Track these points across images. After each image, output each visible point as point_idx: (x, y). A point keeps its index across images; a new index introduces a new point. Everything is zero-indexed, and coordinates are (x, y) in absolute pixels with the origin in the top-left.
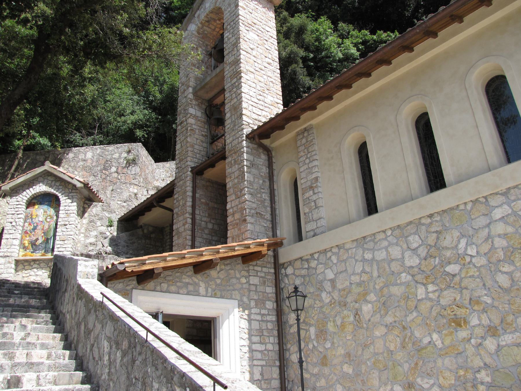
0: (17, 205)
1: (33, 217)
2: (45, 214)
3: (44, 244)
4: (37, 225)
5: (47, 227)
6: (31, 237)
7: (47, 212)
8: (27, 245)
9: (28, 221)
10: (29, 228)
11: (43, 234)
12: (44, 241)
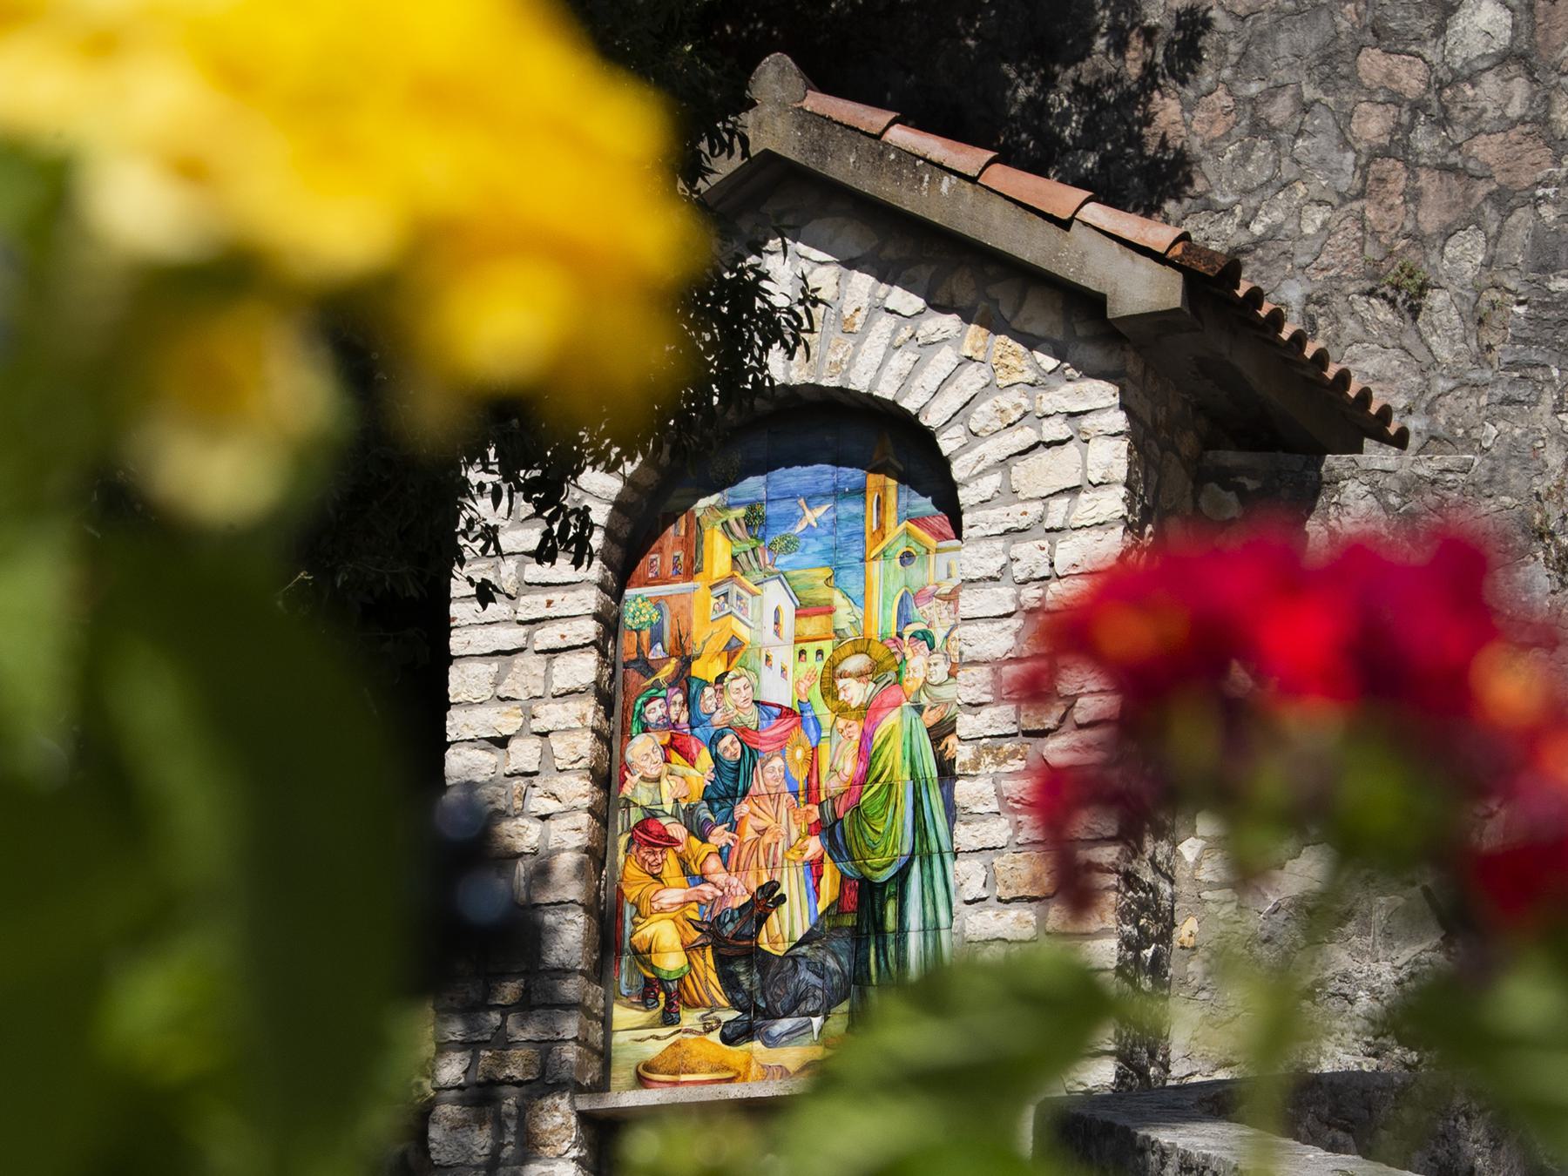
1: (697, 669)
2: (813, 626)
3: (841, 944)
4: (751, 754)
5: (849, 766)
6: (703, 879)
7: (829, 610)
8: (671, 961)
9: (655, 712)
10: (668, 789)
11: (814, 846)
12: (836, 908)
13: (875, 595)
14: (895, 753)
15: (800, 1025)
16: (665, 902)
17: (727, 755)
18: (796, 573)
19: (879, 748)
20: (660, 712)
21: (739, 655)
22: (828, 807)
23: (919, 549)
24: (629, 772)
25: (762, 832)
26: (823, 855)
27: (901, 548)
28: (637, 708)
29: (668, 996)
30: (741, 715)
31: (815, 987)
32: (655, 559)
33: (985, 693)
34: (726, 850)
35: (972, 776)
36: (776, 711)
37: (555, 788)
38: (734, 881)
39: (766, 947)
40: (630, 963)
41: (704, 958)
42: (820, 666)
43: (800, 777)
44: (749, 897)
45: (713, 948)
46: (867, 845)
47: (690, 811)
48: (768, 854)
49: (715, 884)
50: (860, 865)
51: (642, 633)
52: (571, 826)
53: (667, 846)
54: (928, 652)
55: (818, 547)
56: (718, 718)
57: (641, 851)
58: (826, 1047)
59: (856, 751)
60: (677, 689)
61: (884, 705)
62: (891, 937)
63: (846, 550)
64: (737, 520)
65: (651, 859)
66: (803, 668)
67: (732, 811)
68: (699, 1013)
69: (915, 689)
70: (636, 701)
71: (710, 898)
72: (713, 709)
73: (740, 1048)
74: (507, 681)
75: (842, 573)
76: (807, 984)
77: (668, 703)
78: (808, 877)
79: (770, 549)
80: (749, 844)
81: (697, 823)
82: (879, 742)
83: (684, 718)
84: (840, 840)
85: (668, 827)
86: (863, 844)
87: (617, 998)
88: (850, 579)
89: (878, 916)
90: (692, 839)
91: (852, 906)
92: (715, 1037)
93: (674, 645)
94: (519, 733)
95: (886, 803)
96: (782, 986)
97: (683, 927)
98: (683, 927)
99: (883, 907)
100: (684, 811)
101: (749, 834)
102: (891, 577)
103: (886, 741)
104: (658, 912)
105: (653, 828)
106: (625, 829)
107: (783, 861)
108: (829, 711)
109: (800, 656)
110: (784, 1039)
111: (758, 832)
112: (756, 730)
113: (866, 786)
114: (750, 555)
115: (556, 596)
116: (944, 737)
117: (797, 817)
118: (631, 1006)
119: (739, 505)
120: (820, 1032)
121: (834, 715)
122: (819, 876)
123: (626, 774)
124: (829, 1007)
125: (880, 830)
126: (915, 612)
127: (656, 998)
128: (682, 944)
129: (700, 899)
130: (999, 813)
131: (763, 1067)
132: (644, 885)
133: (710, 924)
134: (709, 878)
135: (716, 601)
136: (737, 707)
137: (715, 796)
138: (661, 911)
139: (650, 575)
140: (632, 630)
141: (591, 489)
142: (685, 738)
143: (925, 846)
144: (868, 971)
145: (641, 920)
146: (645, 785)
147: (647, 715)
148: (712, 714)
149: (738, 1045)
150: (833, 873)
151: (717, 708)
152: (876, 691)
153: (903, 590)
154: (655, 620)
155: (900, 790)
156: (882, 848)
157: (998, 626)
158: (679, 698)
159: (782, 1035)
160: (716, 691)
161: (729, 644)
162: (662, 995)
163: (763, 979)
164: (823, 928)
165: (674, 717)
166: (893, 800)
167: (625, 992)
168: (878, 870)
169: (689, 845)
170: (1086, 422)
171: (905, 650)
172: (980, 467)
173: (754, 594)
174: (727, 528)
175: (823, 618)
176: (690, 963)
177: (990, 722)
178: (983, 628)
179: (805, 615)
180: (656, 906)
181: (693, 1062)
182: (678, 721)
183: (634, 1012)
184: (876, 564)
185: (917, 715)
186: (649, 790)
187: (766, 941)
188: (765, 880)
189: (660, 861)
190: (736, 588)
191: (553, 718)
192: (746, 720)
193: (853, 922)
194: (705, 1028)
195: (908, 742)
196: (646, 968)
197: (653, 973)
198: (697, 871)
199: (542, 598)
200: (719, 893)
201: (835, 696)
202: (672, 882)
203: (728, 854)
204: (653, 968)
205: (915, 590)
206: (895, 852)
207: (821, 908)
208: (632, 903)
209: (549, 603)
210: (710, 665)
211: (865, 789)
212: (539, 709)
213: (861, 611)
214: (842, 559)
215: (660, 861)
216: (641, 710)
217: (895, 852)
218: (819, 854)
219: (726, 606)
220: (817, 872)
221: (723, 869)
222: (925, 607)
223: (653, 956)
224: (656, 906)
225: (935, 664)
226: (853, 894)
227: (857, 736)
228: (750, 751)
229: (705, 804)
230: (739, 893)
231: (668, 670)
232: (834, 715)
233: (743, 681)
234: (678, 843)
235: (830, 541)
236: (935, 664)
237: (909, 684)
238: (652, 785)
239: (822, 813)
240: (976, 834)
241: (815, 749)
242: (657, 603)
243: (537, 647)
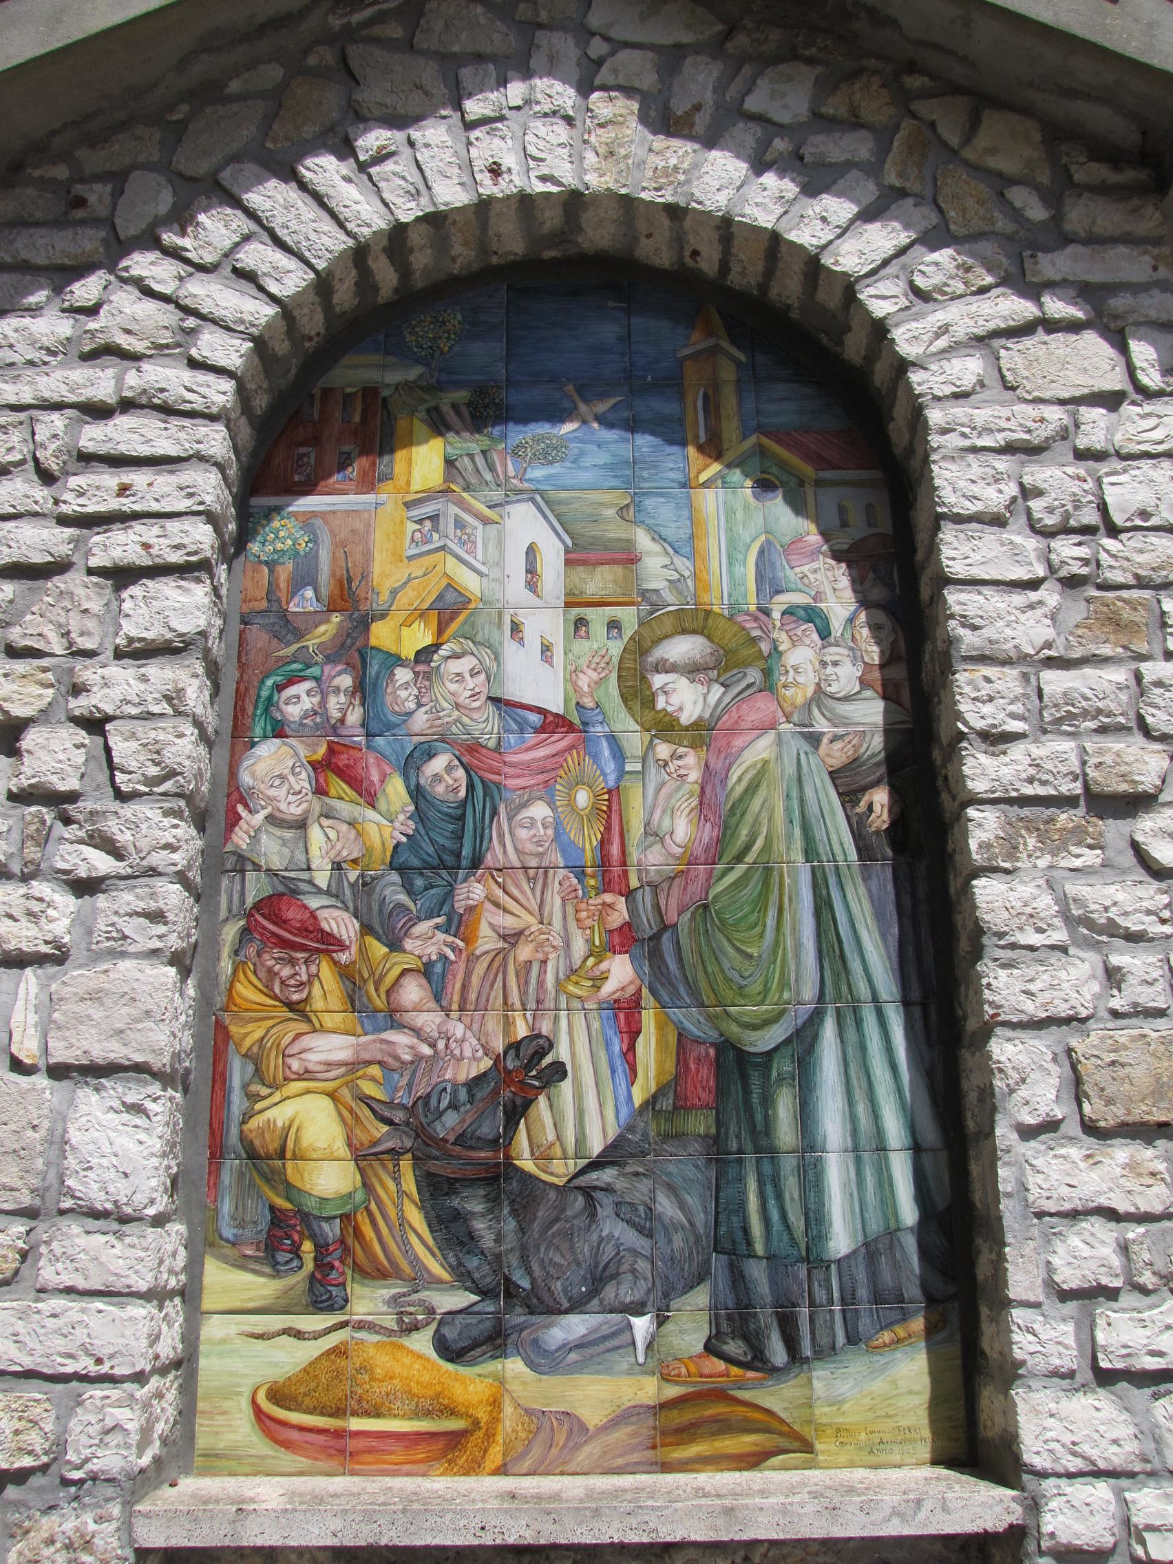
0: (97, 411)
1: (381, 634)
2: (599, 582)
6: (393, 1018)
7: (630, 559)
13: (713, 542)
14: (772, 810)
15: (606, 1330)
16: (313, 1058)
17: (440, 789)
18: (564, 494)
19: (741, 799)
20: (307, 703)
21: (460, 619)
22: (645, 899)
23: (785, 477)
24: (246, 806)
25: (513, 938)
26: (640, 989)
28: (265, 693)
29: (321, 1249)
30: (466, 720)
31: (635, 1253)
32: (305, 455)
33: (1013, 716)
34: (438, 968)
35: (1007, 872)
36: (535, 718)
37: (112, 827)
38: (459, 1030)
39: (527, 1165)
40: (241, 1175)
41: (397, 1180)
42: (615, 649)
43: (588, 841)
44: (487, 1063)
45: (415, 1158)
46: (729, 980)
47: (366, 885)
48: (527, 982)
49: (417, 1032)
50: (717, 1016)
51: (279, 568)
52: (141, 906)
53: (318, 951)
54: (819, 642)
55: (603, 458)
56: (420, 720)
57: (266, 956)
58: (666, 1378)
59: (695, 802)
60: (340, 667)
61: (743, 725)
62: (788, 1163)
63: (654, 467)
64: (455, 406)
65: (286, 972)
66: (582, 647)
67: (450, 894)
68: (386, 1292)
69: (799, 700)
70: (262, 682)
71: (407, 1058)
72: (412, 705)
73: (477, 1369)
74: (29, 617)
75: (649, 502)
76: (618, 1246)
77: (323, 689)
78: (611, 1032)
79: (515, 454)
80: (488, 959)
81: (381, 910)
82: (739, 790)
83: (354, 716)
84: (672, 965)
85: (322, 914)
86: (720, 977)
87: (212, 1245)
88: (663, 510)
89: (759, 1117)
90: (371, 941)
91: (704, 1095)
92: (422, 1342)
93: (337, 592)
94: (43, 716)
95: (761, 902)
96: (565, 1246)
97: (351, 1111)
98: (351, 1111)
99: (768, 1101)
100: (352, 885)
101: (487, 941)
102: (740, 515)
103: (752, 788)
104: (300, 1078)
105: (291, 914)
106: (235, 910)
107: (556, 1000)
108: (638, 728)
109: (577, 628)
110: (573, 1356)
111: (504, 938)
112: (497, 749)
113: (720, 867)
114: (480, 460)
115: (138, 478)
116: (864, 789)
117: (584, 915)
118: (241, 1263)
119: (458, 385)
120: (649, 1347)
121: (647, 736)
122: (633, 1033)
123: (240, 808)
124: (666, 1295)
125: (754, 951)
126: (791, 575)
127: (296, 1251)
128: (350, 1145)
129: (390, 1060)
130: (1064, 949)
131: (529, 1412)
132: (271, 1022)
133: (411, 1110)
134: (408, 1017)
135: (418, 527)
136: (457, 706)
137: (416, 862)
138: (306, 1075)
139: (296, 478)
140: (260, 562)
141: (218, 313)
142: (359, 755)
143: (844, 988)
144: (746, 1231)
145: (264, 1091)
146: (278, 832)
147: (283, 707)
148: (410, 714)
149: (473, 1363)
150: (660, 1027)
151: (419, 705)
152: (727, 699)
153: (763, 538)
154: (302, 548)
155: (787, 881)
156: (758, 987)
157: (1018, 599)
158: (346, 681)
159: (567, 1347)
160: (416, 674)
161: (440, 597)
162: (307, 1246)
163: (522, 1230)
164: (645, 1134)
165: (335, 714)
166: (774, 897)
167: (228, 1233)
168: (755, 1027)
169: (363, 950)
170: (1118, 303)
171: (775, 635)
172: (942, 343)
173: (486, 521)
175: (619, 570)
176: (365, 1185)
177: (1032, 771)
178: (997, 601)
179: (584, 563)
180: (295, 1065)
181: (380, 1389)
182: (342, 721)
183: (248, 1277)
184: (710, 494)
185: (805, 747)
186: (284, 842)
187: (527, 1153)
188: (522, 1031)
189: (304, 978)
190: (454, 510)
191: (116, 693)
192: (476, 729)
193: (709, 1127)
194: (400, 1321)
195: (795, 793)
196: (273, 1188)
197: (288, 1199)
198: (379, 1003)
199: (109, 480)
200: (426, 1050)
202: (329, 1020)
203: (444, 976)
204: (289, 1190)
205: (787, 540)
206: (786, 996)
207: (639, 1095)
208: (245, 1056)
209: (123, 490)
210: (405, 630)
211: (716, 873)
212: (88, 673)
213: (688, 563)
214: (645, 480)
215: (304, 978)
216: (270, 697)
217: (786, 996)
218: (631, 990)
219: (436, 536)
220: (628, 1024)
221: (433, 1005)
222: (805, 569)
223: (289, 1164)
224: (295, 1065)
225: (835, 664)
226: (704, 1072)
227: (694, 776)
228: (483, 782)
229: (395, 877)
230: (468, 1053)
231: (326, 631)
232: (647, 736)
233: (465, 664)
234: (343, 947)
236: (835, 664)
237: (789, 693)
238: (289, 834)
239: (632, 911)
240: (1032, 987)
241: (614, 793)
243: (94, 562)
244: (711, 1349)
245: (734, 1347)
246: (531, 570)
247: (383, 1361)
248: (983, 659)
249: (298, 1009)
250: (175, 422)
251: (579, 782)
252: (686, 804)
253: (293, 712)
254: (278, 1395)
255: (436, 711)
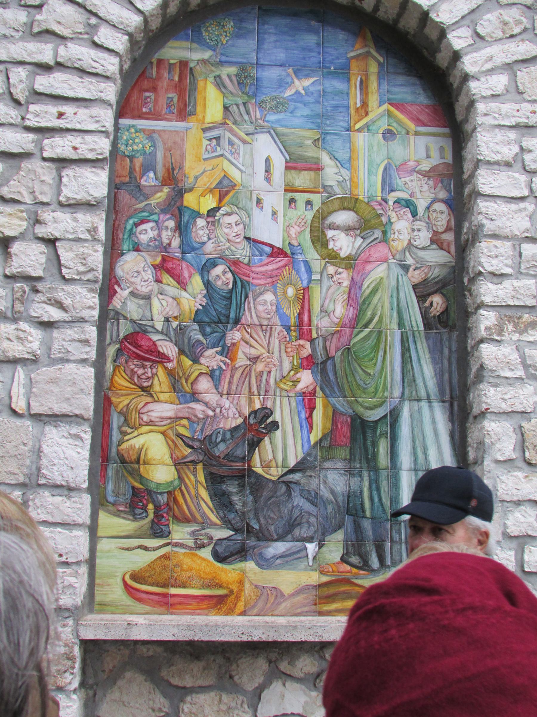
0: (45, 68)
1: (189, 200)
6: (194, 397)
7: (318, 169)
13: (361, 162)
14: (383, 303)
15: (294, 549)
16: (154, 415)
17: (219, 283)
18: (286, 130)
19: (368, 297)
20: (152, 234)
21: (231, 194)
22: (319, 344)
23: (399, 129)
24: (119, 286)
25: (254, 360)
26: (315, 388)
27: (383, 125)
28: (129, 227)
29: (157, 508)
30: (233, 248)
31: (310, 514)
32: (148, 97)
33: (507, 265)
34: (217, 373)
35: (497, 341)
36: (268, 249)
37: (61, 296)
38: (227, 404)
39: (259, 470)
40: (117, 471)
41: (195, 476)
42: (310, 215)
43: (293, 313)
44: (240, 420)
45: (204, 465)
46: (358, 385)
47: (181, 330)
48: (261, 382)
49: (206, 404)
50: (352, 402)
51: (136, 160)
52: (77, 337)
53: (157, 362)
54: (412, 219)
55: (306, 112)
56: (210, 247)
57: (130, 363)
58: (322, 573)
59: (346, 297)
60: (168, 216)
61: (372, 259)
62: (383, 474)
63: (334, 119)
64: (229, 76)
65: (141, 371)
66: (292, 213)
67: (223, 336)
68: (189, 529)
69: (400, 248)
70: (127, 221)
71: (201, 416)
72: (205, 239)
73: (232, 566)
74: (12, 182)
75: (329, 138)
76: (301, 510)
78: (301, 408)
79: (261, 106)
80: (242, 369)
81: (189, 343)
82: (368, 292)
83: (176, 243)
84: (332, 377)
85: (159, 343)
86: (354, 383)
87: (102, 505)
89: (370, 451)
90: (183, 358)
91: (344, 440)
92: (206, 553)
93: (166, 175)
94: (21, 237)
95: (376, 348)
96: (276, 510)
97: (173, 441)
98: (173, 441)
99: (375, 444)
100: (175, 330)
101: (241, 361)
102: (375, 148)
103: (375, 291)
104: (147, 424)
105: (143, 342)
106: (114, 339)
107: (275, 390)
108: (319, 257)
109: (290, 204)
110: (278, 561)
111: (250, 359)
112: (248, 265)
113: (356, 330)
114: (242, 108)
115: (69, 109)
116: (429, 295)
117: (289, 350)
118: (118, 514)
120: (315, 558)
121: (324, 262)
122: (311, 408)
123: (116, 287)
124: (323, 534)
125: (371, 372)
126: (399, 182)
127: (145, 509)
128: (172, 458)
129: (193, 417)
130: (522, 379)
131: (257, 587)
132: (133, 397)
133: (202, 442)
134: (201, 396)
135: (209, 142)
136: (229, 241)
137: (207, 320)
138: (150, 423)
139: (144, 110)
140: (125, 156)
141: (108, 18)
142: (178, 262)
143: (414, 392)
144: (362, 505)
145: (129, 430)
146: (136, 300)
147: (138, 235)
148: (204, 243)
149: (230, 563)
150: (325, 406)
151: (209, 239)
152: (364, 245)
153: (386, 161)
154: (148, 150)
155: (389, 338)
156: (372, 389)
157: (514, 207)
158: (171, 224)
159: (276, 557)
160: (208, 222)
161: (220, 182)
162: (150, 506)
163: (255, 501)
164: (316, 458)
165: (166, 241)
166: (382, 346)
167: (111, 499)
168: (371, 409)
169: (179, 362)
171: (390, 213)
172: (488, 66)
173: (245, 142)
174: (219, 84)
175: (312, 173)
176: (180, 477)
177: (513, 293)
178: (504, 207)
179: (295, 169)
180: (145, 418)
181: (185, 575)
182: (169, 244)
183: (120, 521)
184: (361, 135)
185: (402, 272)
186: (139, 306)
187: (259, 465)
188: (257, 405)
189: (150, 375)
190: (228, 135)
191: (61, 226)
192: (238, 253)
193: (346, 455)
194: (196, 543)
195: (395, 295)
196: (133, 478)
197: (142, 485)
198: (188, 389)
199: (53, 109)
200: (211, 413)
201: (325, 244)
202: (162, 397)
203: (220, 377)
204: (141, 479)
205: (398, 163)
206: (385, 394)
207: (314, 438)
208: (120, 412)
209: (61, 115)
210: (202, 199)
211: (355, 333)
212: (46, 215)
213: (348, 173)
214: (328, 126)
215: (150, 375)
216: (131, 229)
217: (385, 394)
218: (311, 388)
219: (218, 149)
220: (309, 404)
221: (214, 391)
222: (407, 179)
223: (142, 467)
224: (145, 418)
225: (419, 230)
226: (345, 429)
227: (346, 283)
228: (241, 281)
229: (196, 326)
230: (231, 415)
232: (324, 262)
234: (169, 360)
235: (318, 109)
236: (419, 230)
237: (395, 244)
238: (142, 302)
239: (313, 349)
240: (506, 397)
241: (306, 290)
242: (150, 134)
243: (46, 155)
244: (343, 560)
245: (355, 560)
246: (267, 171)
247: (187, 562)
248: (495, 236)
249: (147, 390)
250: (87, 79)
251: (289, 283)
252: (341, 296)
253: (144, 238)
254: (135, 577)
255: (218, 243)
